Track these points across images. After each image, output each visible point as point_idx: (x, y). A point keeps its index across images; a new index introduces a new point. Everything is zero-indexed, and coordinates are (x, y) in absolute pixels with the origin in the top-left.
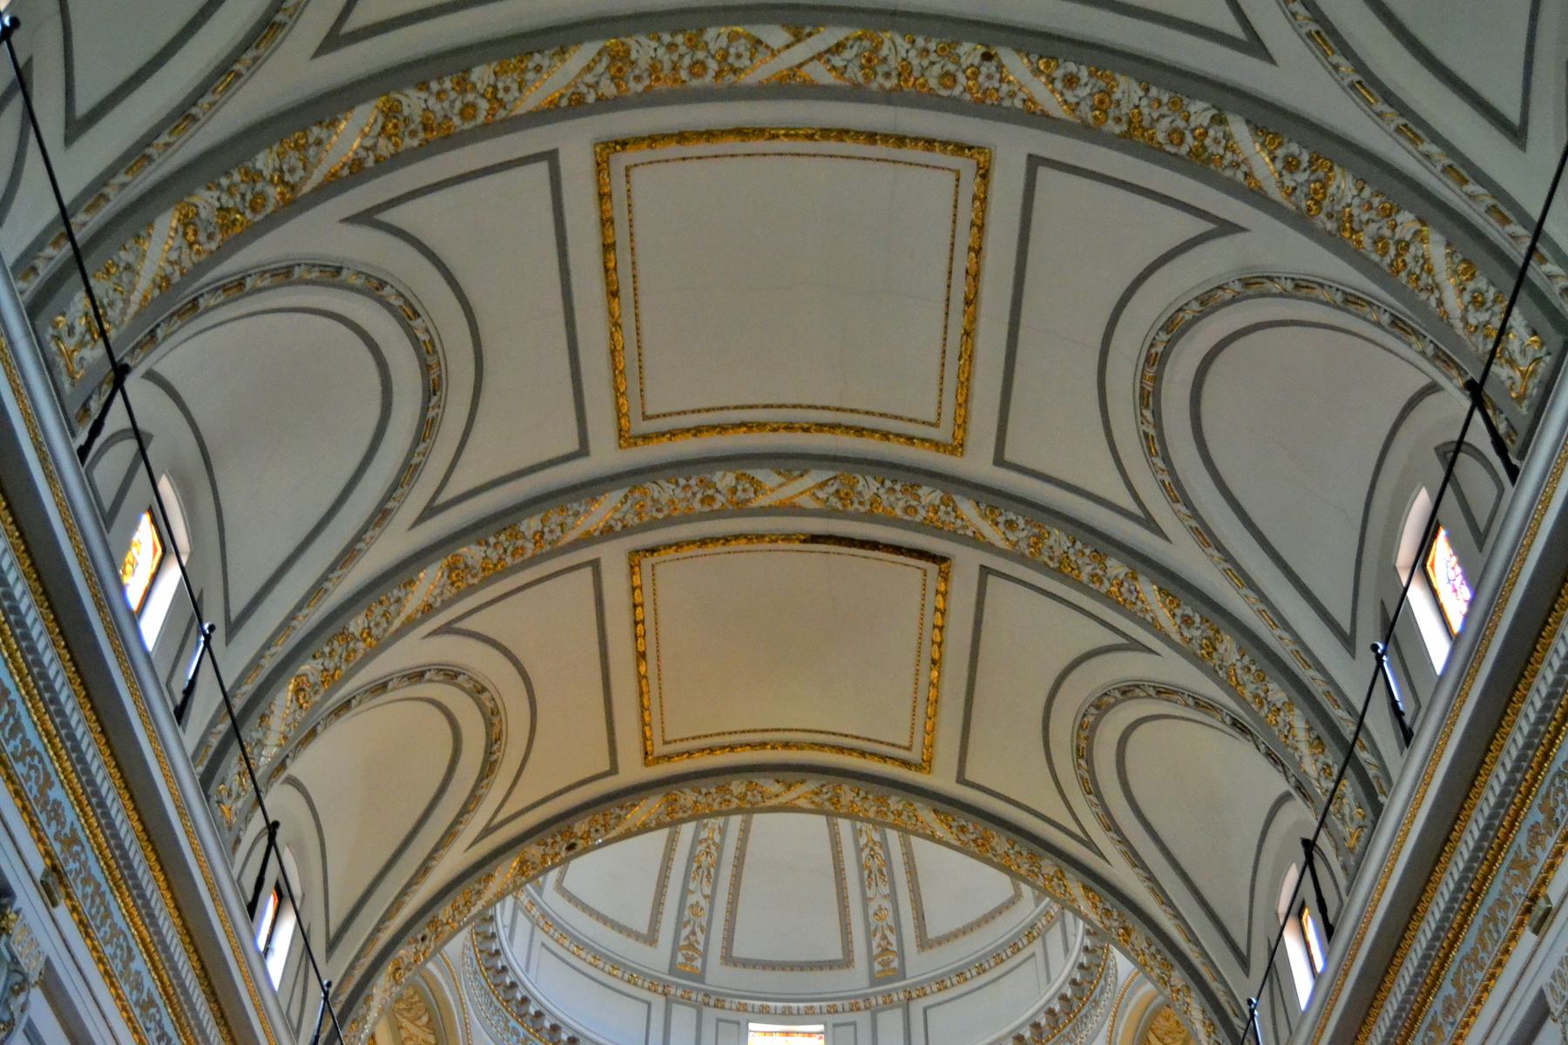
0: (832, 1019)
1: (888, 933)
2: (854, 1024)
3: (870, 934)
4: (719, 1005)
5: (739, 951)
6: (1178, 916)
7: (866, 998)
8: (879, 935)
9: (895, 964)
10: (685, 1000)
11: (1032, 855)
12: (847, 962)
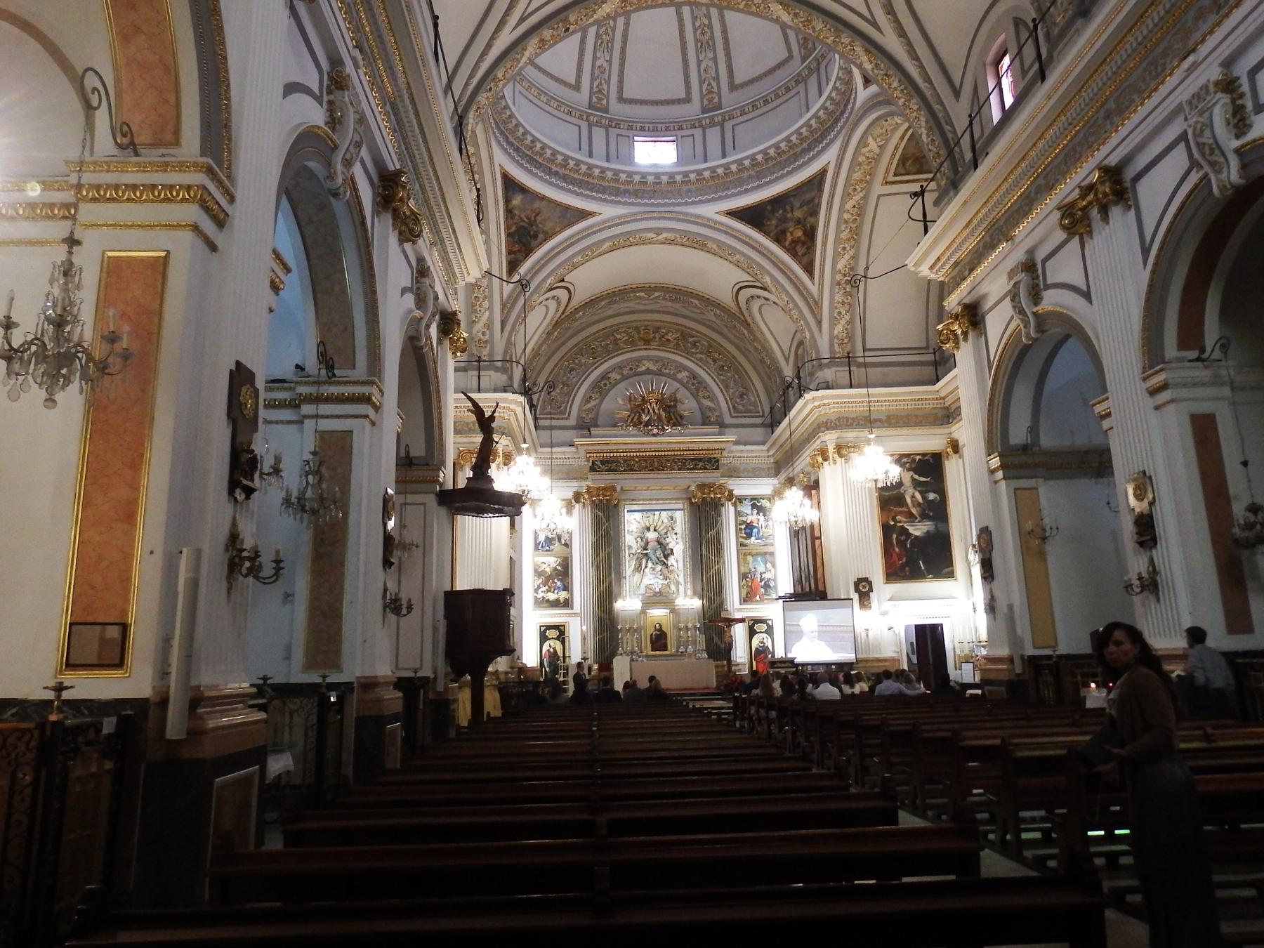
0: (680, 133)
1: (712, 81)
2: (693, 135)
3: (701, 82)
4: (617, 126)
5: (625, 95)
6: (921, 67)
7: (700, 120)
8: (706, 84)
9: (716, 100)
10: (599, 124)
11: (836, 29)
12: (688, 100)
